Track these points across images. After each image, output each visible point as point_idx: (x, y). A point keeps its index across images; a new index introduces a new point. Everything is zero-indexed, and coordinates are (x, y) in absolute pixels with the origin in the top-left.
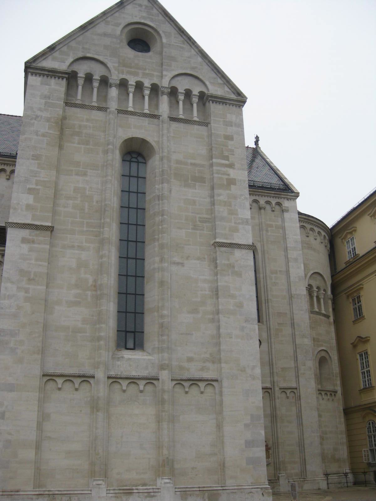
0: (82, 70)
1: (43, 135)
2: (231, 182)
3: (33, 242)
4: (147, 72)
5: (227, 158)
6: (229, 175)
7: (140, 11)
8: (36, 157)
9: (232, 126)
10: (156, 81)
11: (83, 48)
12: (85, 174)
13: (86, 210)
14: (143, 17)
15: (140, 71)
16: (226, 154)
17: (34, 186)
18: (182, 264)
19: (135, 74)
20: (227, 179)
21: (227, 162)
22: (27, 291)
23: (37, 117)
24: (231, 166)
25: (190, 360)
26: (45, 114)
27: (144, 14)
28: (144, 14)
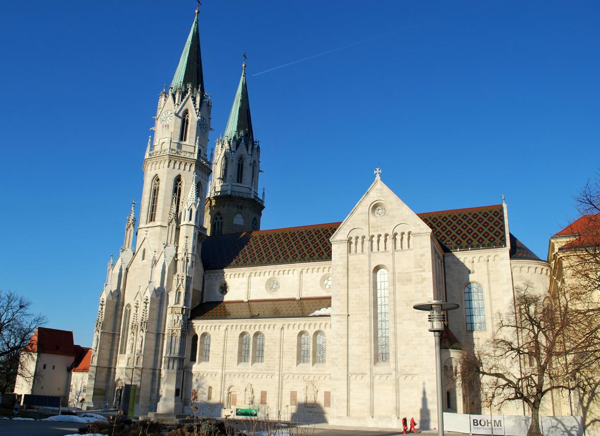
0: (353, 235)
1: (341, 273)
2: (424, 279)
3: (341, 321)
4: (383, 228)
5: (421, 267)
6: (422, 276)
7: (377, 193)
8: (339, 284)
9: (424, 248)
10: (387, 232)
11: (353, 224)
12: (359, 288)
13: (361, 304)
14: (379, 197)
15: (379, 229)
16: (421, 264)
17: (339, 297)
18: (402, 323)
19: (377, 231)
20: (422, 278)
21: (421, 269)
22: (340, 342)
23: (337, 265)
24: (424, 271)
25: (406, 366)
26: (340, 263)
27: (379, 195)
28: (379, 195)
